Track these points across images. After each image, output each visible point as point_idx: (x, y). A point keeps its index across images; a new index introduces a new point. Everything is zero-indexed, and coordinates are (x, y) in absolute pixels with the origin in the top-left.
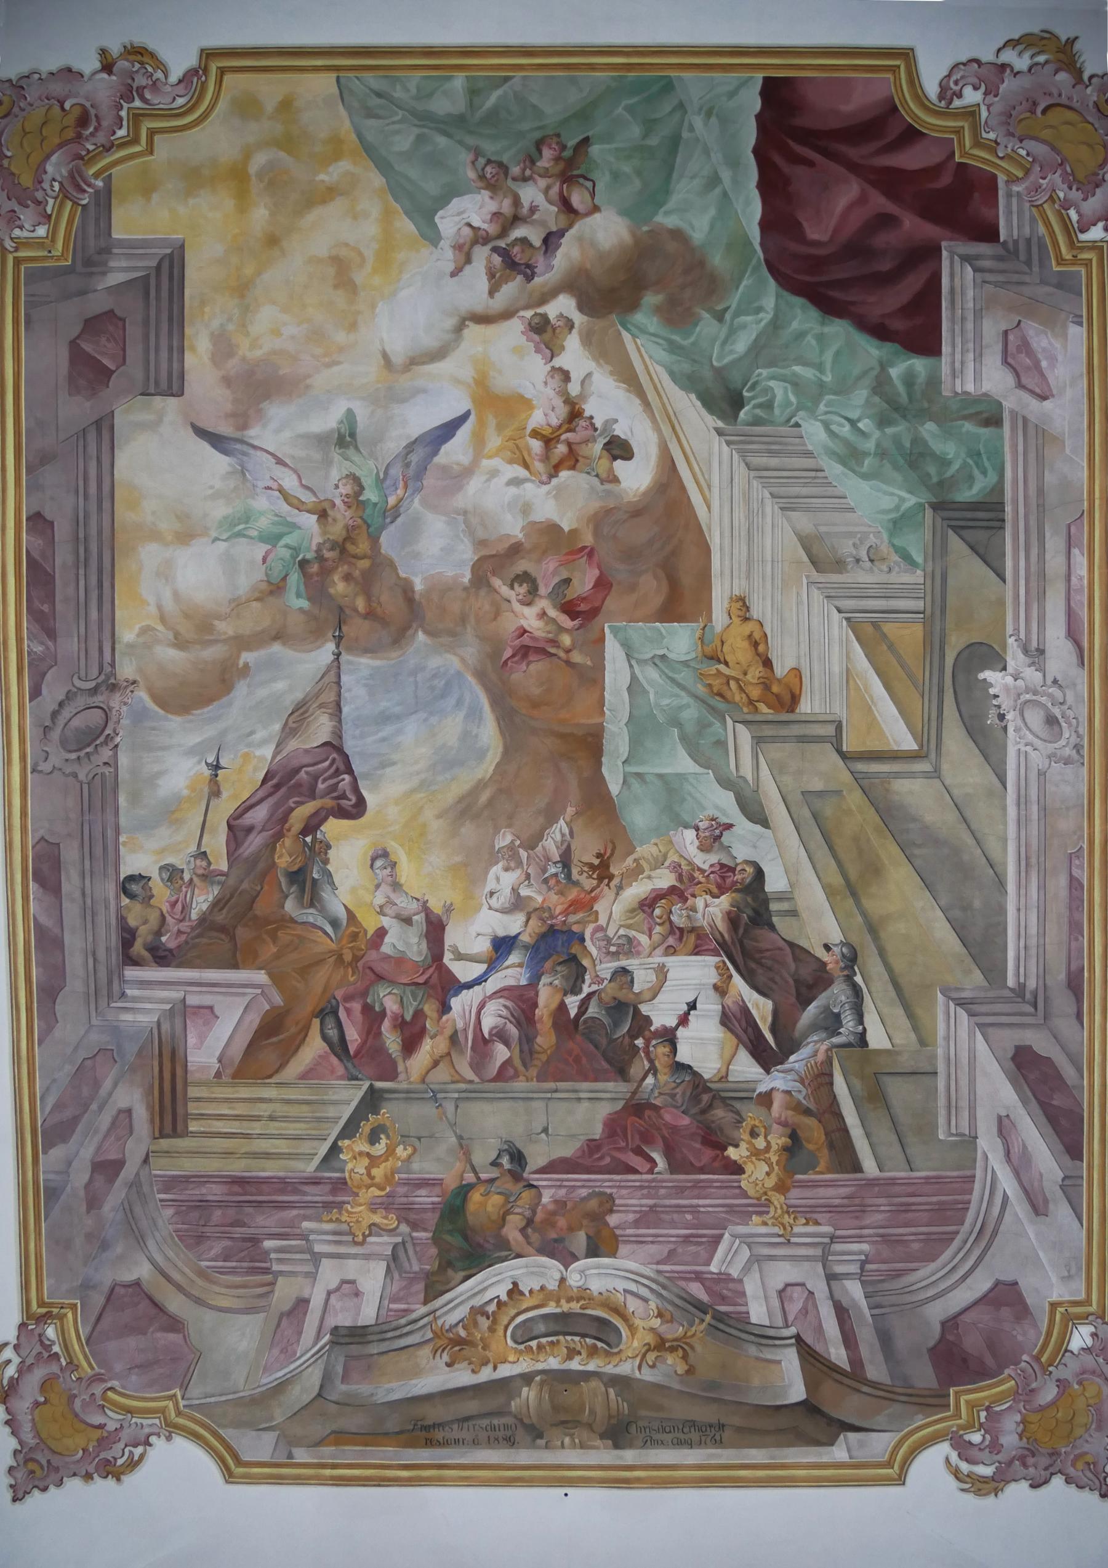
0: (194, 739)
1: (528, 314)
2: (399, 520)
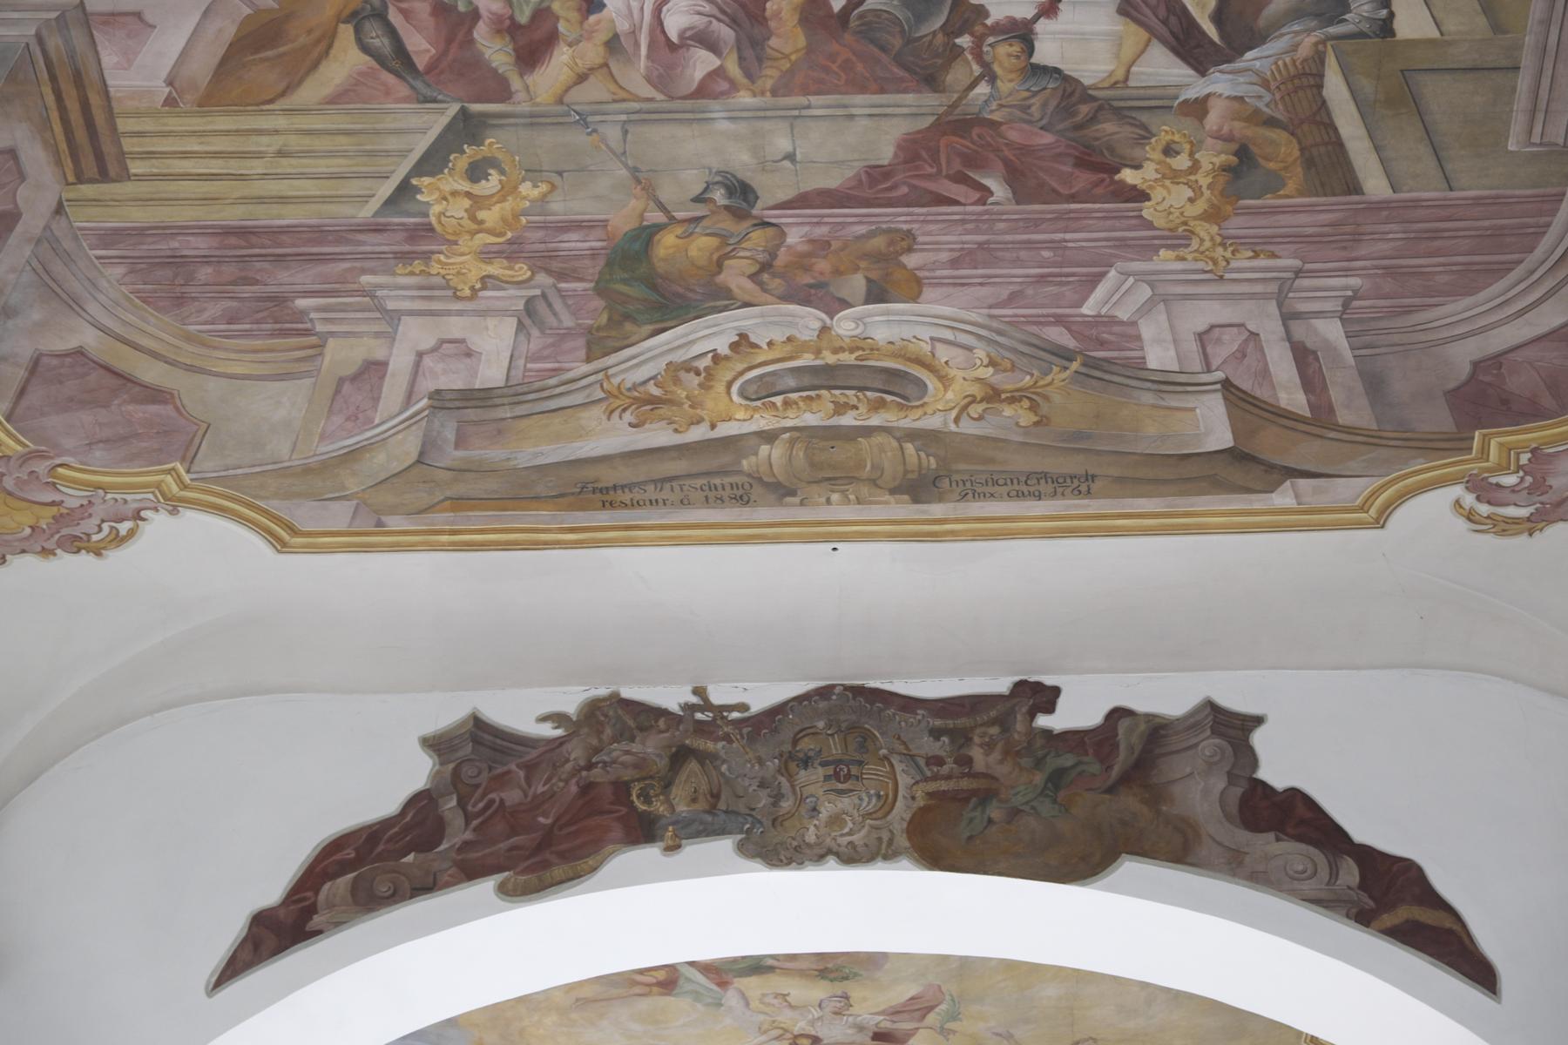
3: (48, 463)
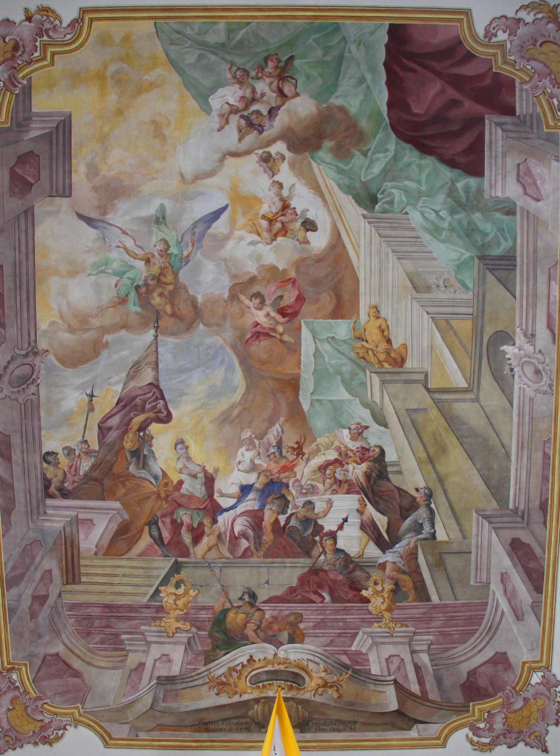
0: (79, 381)
1: (260, 152)
2: (190, 264)
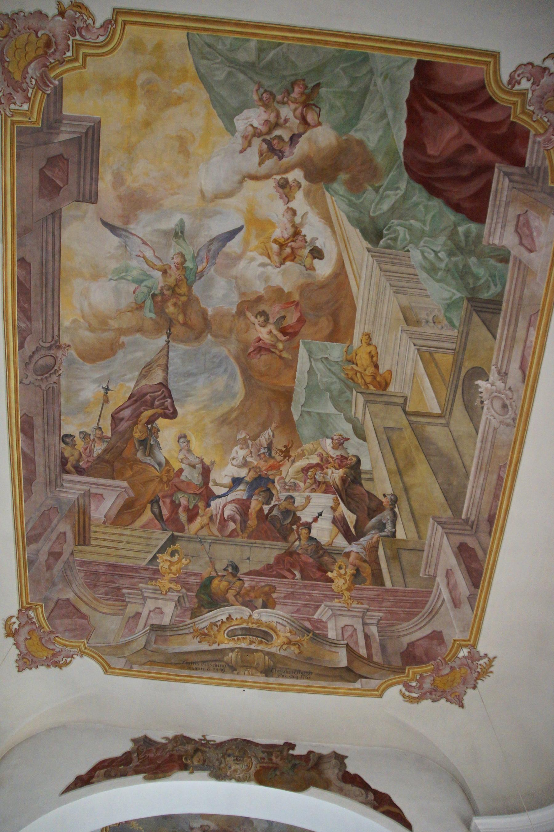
0: (97, 375)
1: (278, 177)
2: (203, 279)
3: (54, 635)
